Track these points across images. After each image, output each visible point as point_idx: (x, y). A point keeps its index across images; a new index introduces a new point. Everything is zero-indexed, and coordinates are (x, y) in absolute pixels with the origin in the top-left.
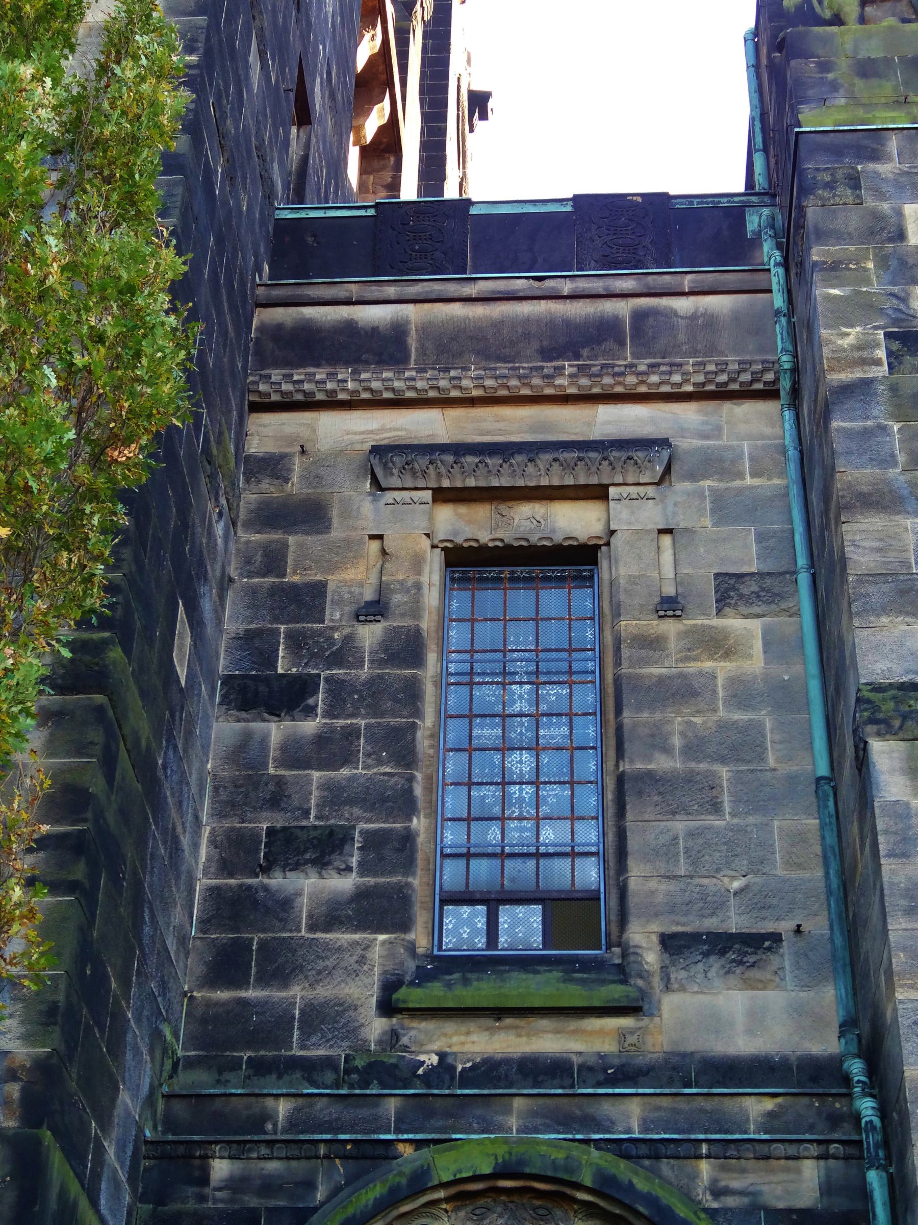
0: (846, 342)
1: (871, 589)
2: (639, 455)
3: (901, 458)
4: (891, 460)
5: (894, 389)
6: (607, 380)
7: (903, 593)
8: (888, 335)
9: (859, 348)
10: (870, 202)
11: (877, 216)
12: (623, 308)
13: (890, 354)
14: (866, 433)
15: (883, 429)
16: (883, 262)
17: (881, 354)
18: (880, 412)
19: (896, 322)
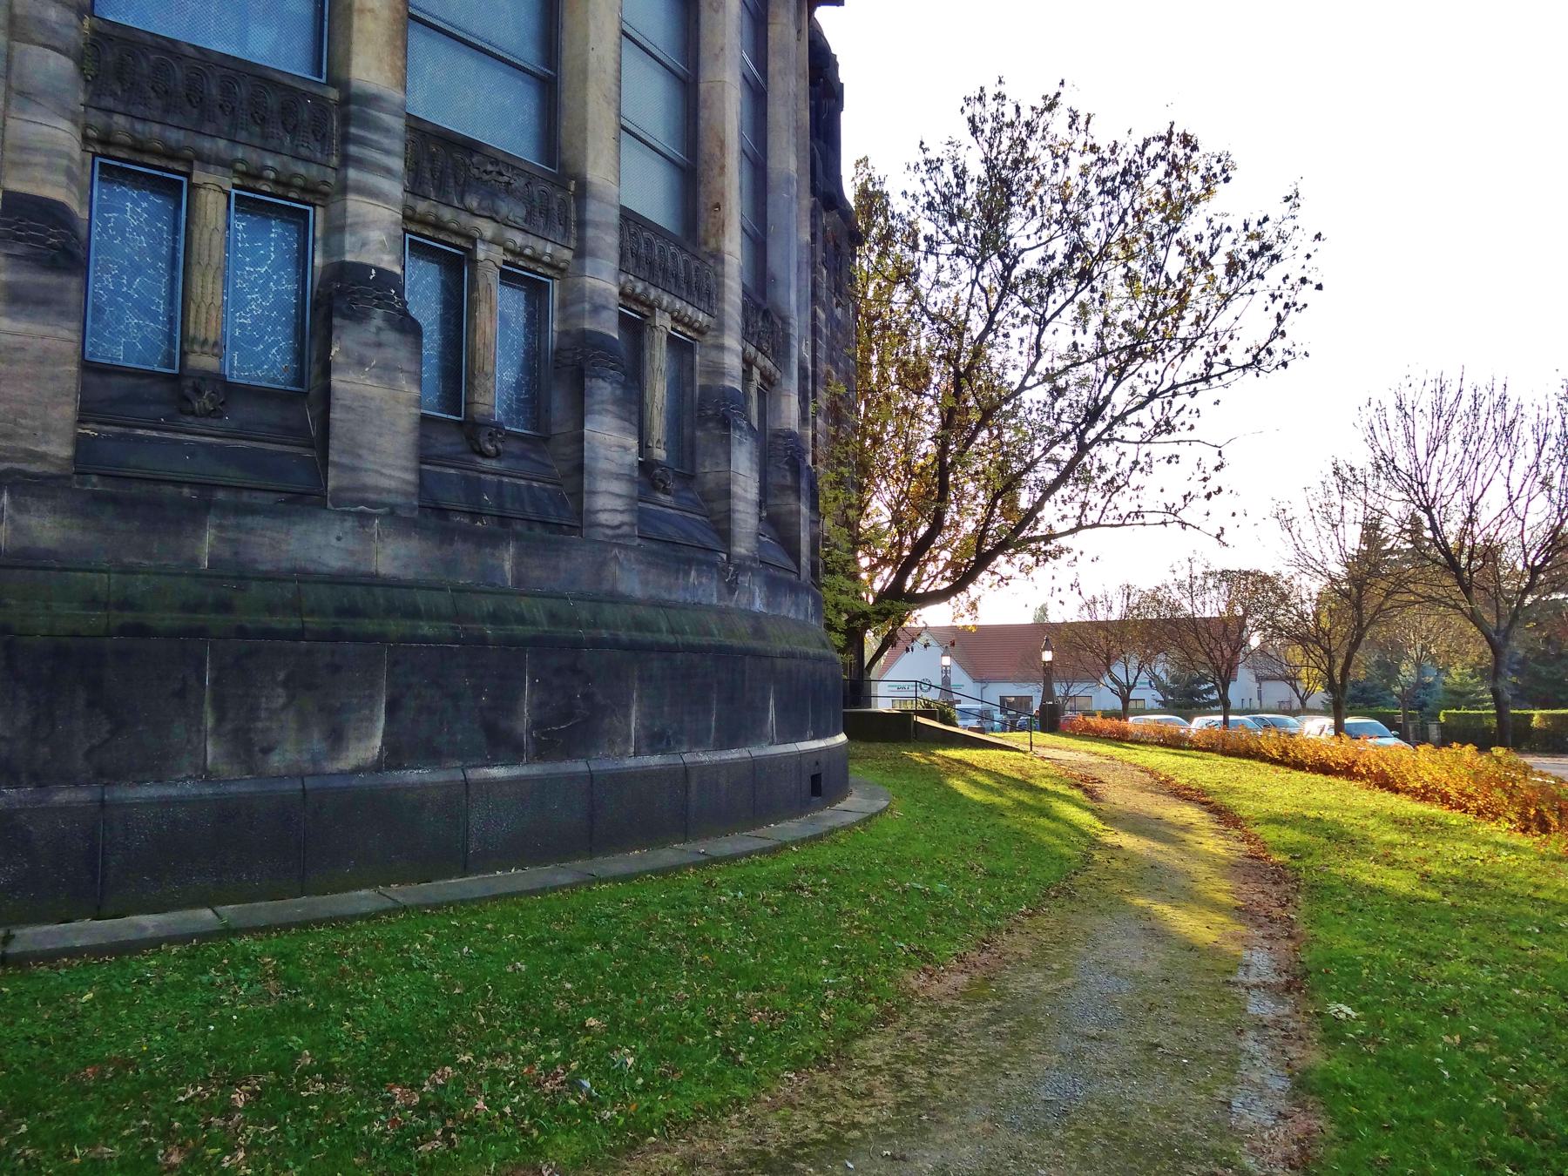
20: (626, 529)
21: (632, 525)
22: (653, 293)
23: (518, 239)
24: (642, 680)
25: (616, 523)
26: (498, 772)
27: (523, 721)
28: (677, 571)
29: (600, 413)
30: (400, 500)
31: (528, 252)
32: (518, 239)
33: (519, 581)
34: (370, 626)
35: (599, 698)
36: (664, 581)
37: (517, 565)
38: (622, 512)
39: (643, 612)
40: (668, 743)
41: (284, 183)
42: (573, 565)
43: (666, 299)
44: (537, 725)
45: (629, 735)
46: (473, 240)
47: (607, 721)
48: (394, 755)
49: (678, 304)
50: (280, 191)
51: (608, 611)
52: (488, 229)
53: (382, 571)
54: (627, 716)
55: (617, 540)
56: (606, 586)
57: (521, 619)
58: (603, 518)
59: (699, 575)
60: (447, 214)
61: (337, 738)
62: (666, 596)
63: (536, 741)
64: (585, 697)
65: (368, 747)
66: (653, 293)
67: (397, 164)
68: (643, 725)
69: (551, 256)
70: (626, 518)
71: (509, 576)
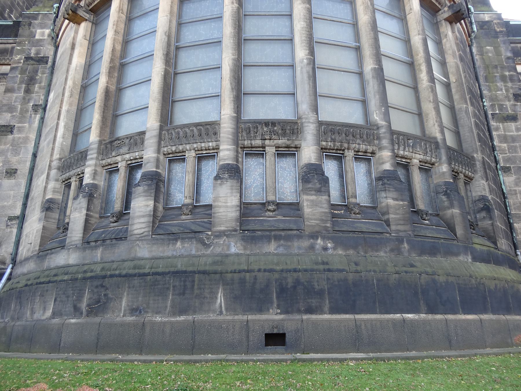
0: (16, 59)
1: (4, 107)
2: (5, 76)
3: (18, 82)
4: (16, 83)
5: (22, 68)
6: (3, 61)
7: (9, 108)
8: (25, 57)
9: (18, 60)
10: (31, 29)
11: (32, 32)
12: (9, 46)
13: (24, 61)
14: (14, 77)
15: (17, 76)
16: (29, 42)
17: (22, 61)
18: (17, 72)
19: (27, 55)
20: (146, 234)
21: (149, 231)
22: (181, 148)
23: (127, 156)
24: (129, 287)
25: (142, 232)
26: (73, 321)
27: (84, 306)
28: (169, 244)
29: (138, 197)
30: (78, 242)
31: (132, 158)
32: (127, 156)
33: (101, 259)
34: (59, 278)
35: (110, 296)
36: (161, 249)
37: (102, 253)
38: (144, 228)
39: (142, 262)
40: (140, 312)
41: (288, 147)
42: (121, 251)
43: (188, 147)
44: (88, 305)
45: (121, 309)
46: (118, 163)
47: (112, 303)
48: (54, 315)
49: (195, 145)
50: (287, 149)
51: (127, 264)
52: (119, 158)
53: (70, 263)
54: (121, 302)
55: (141, 238)
56: (133, 255)
57: (92, 271)
58: (136, 232)
59: (182, 243)
60: (109, 161)
61: (45, 309)
62: (161, 255)
63: (87, 311)
64: (105, 295)
65: (49, 313)
66: (181, 148)
67: (95, 156)
68: (128, 305)
69: (138, 155)
70: (146, 230)
71: (99, 258)
